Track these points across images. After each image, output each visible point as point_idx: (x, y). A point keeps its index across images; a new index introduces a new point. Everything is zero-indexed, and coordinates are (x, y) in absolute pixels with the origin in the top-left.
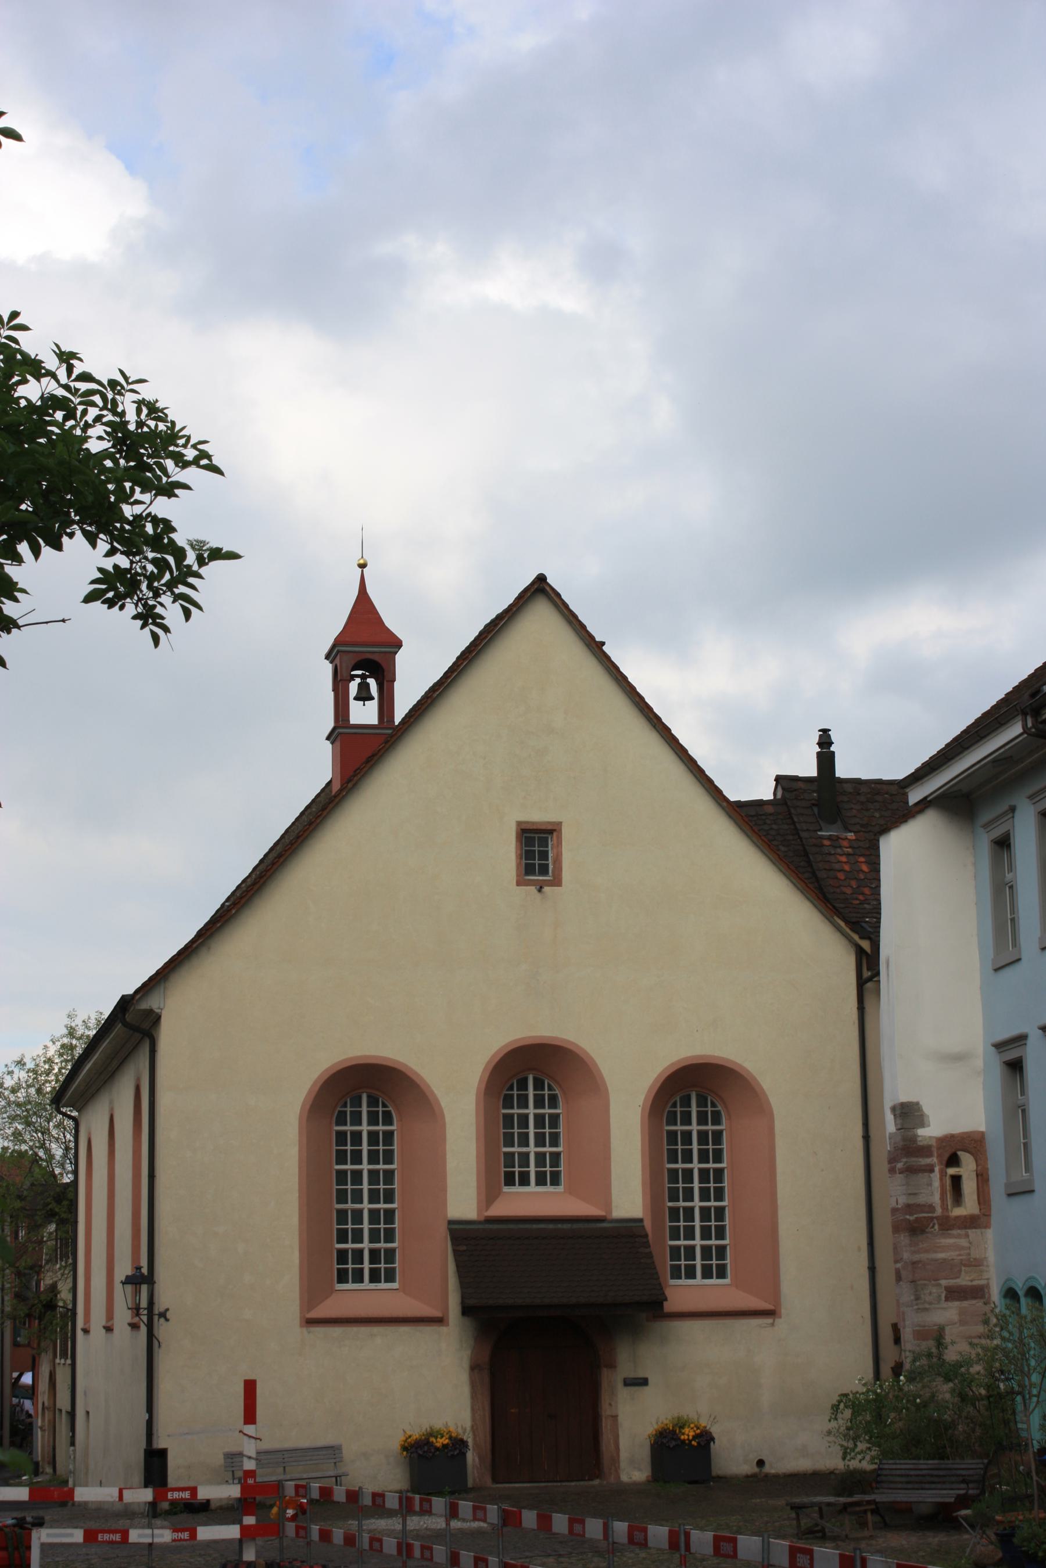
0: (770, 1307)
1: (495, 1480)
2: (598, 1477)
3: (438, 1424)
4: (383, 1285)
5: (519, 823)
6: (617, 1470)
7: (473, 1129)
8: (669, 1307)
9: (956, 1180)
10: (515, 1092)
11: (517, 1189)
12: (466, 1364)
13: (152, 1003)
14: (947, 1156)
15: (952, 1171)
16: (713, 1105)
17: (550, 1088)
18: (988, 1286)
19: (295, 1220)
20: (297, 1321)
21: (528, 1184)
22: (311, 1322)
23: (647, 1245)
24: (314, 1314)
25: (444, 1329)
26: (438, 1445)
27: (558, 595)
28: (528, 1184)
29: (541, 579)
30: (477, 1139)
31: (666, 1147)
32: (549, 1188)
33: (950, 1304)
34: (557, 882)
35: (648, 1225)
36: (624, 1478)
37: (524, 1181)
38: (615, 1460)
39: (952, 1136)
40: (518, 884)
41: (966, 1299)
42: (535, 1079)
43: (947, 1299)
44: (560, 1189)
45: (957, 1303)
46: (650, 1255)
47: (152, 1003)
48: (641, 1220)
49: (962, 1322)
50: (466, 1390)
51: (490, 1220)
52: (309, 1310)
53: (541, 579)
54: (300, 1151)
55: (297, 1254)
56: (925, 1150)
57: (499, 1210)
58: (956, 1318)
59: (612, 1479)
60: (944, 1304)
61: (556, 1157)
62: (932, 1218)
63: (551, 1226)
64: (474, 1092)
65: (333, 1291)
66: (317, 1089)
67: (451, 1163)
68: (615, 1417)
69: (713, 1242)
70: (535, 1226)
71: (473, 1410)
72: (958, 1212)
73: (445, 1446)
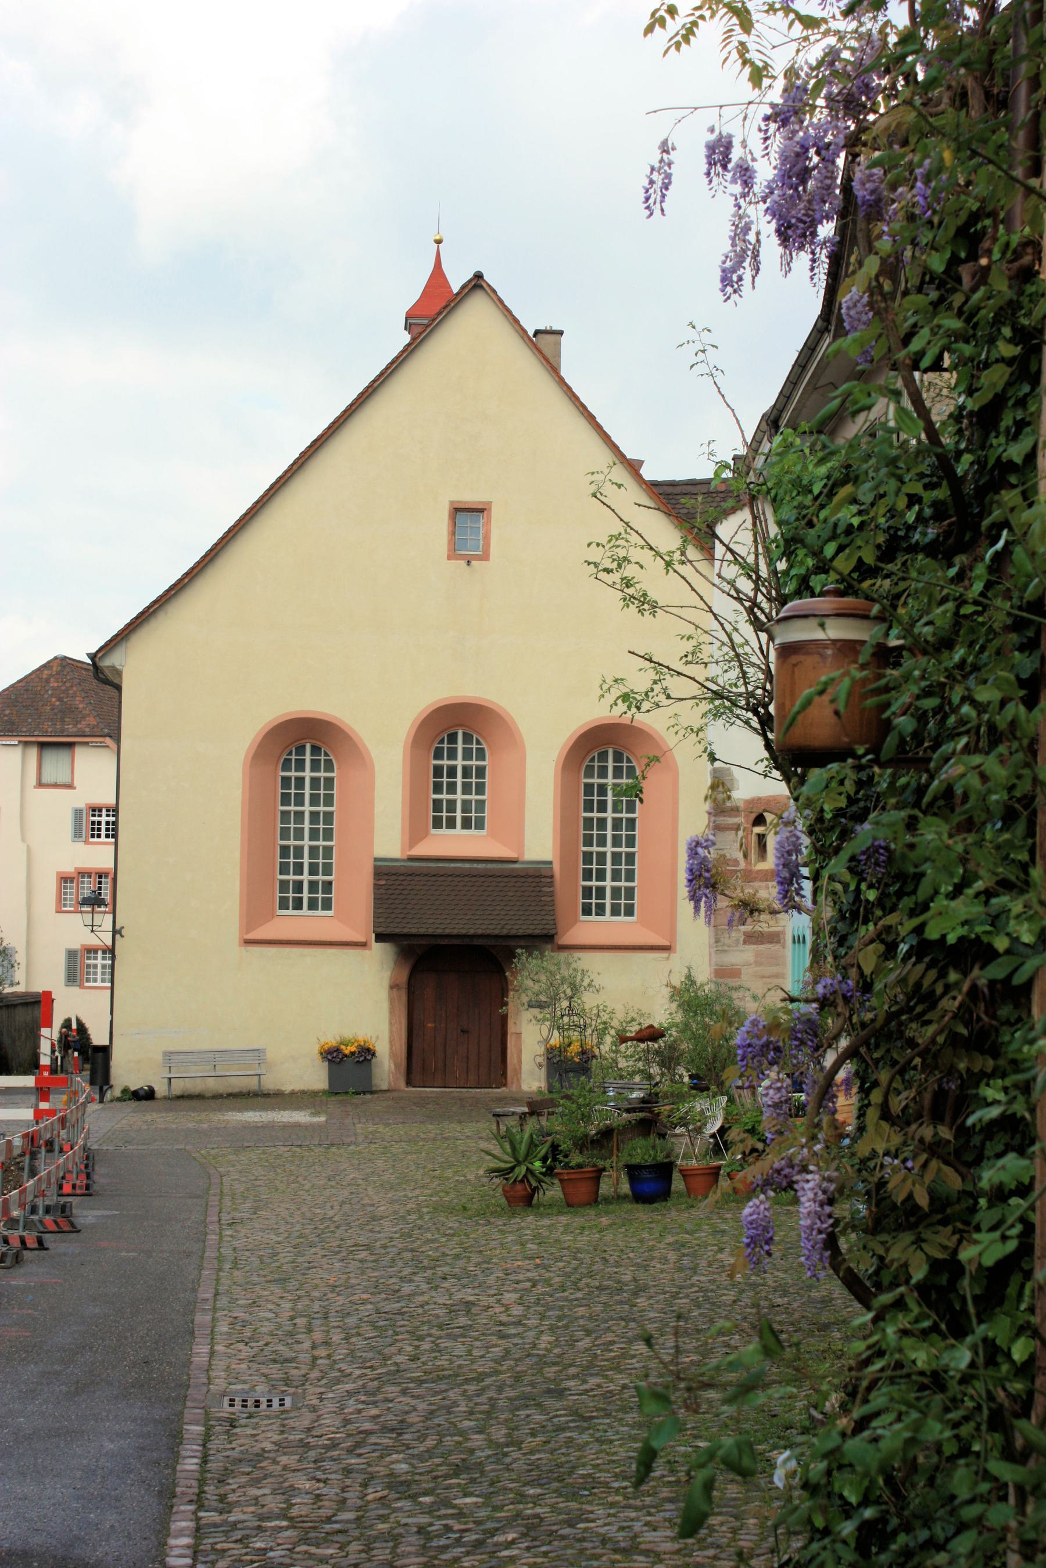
0: (666, 943)
1: (409, 1082)
2: (505, 1085)
3: (348, 1035)
4: (320, 912)
5: (452, 503)
6: (519, 1080)
7: (400, 777)
8: (565, 939)
9: (761, 838)
10: (445, 745)
11: (444, 831)
12: (386, 984)
13: (113, 660)
14: (753, 816)
15: (758, 830)
16: (629, 761)
17: (478, 742)
18: (783, 932)
19: (237, 855)
20: (237, 942)
21: (454, 827)
22: (248, 942)
23: (551, 884)
24: (252, 936)
25: (366, 952)
26: (347, 1052)
27: (494, 292)
28: (454, 827)
29: (479, 276)
30: (404, 786)
31: (583, 797)
32: (473, 832)
33: (747, 947)
34: (485, 557)
35: (556, 868)
36: (525, 1087)
37: (451, 824)
38: (518, 1071)
39: (759, 799)
40: (449, 558)
41: (762, 943)
42: (464, 734)
43: (745, 943)
44: (483, 832)
45: (754, 947)
46: (552, 894)
47: (113, 660)
48: (551, 863)
49: (758, 963)
50: (385, 1005)
51: (411, 859)
52: (247, 932)
53: (479, 276)
54: (243, 793)
55: (238, 883)
56: (735, 811)
57: (424, 849)
58: (752, 959)
59: (514, 1088)
60: (742, 947)
61: (481, 804)
62: (736, 871)
63: (467, 865)
64: (402, 744)
65: (273, 915)
66: (260, 738)
67: (379, 808)
68: (519, 1035)
69: (623, 884)
70: (453, 865)
71: (391, 1023)
72: (762, 866)
73: (353, 1053)
